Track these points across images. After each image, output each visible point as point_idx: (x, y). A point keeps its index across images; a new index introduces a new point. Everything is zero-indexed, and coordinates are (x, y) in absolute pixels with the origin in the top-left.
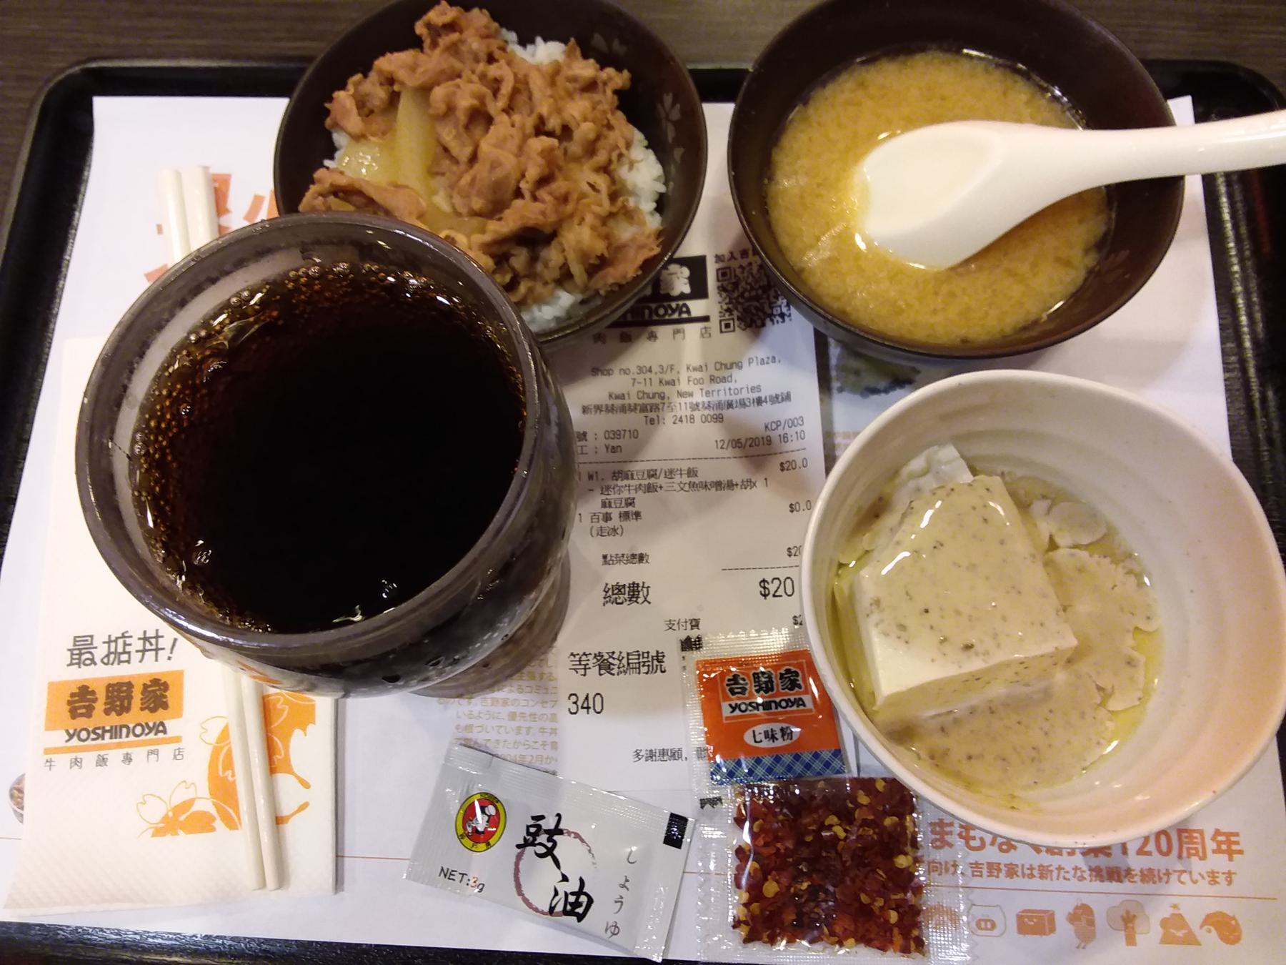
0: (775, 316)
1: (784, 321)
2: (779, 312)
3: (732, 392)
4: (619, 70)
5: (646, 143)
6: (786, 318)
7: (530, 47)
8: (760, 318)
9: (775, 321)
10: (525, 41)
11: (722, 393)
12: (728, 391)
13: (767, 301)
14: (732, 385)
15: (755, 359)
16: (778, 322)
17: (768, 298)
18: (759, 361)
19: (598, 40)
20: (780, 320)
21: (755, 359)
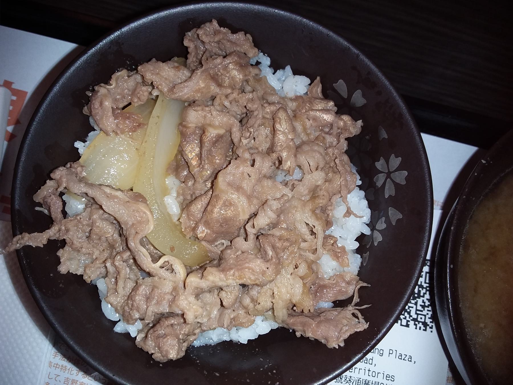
0: (419, 322)
1: (425, 330)
2: (423, 320)
3: (370, 373)
4: (355, 119)
5: (360, 183)
6: (428, 327)
7: (279, 73)
8: (405, 318)
9: (418, 326)
10: (276, 66)
11: (362, 372)
12: (367, 372)
13: (415, 306)
14: (372, 368)
15: (395, 352)
16: (420, 328)
17: (416, 304)
18: (398, 355)
19: (341, 86)
20: (423, 328)
21: (395, 352)
